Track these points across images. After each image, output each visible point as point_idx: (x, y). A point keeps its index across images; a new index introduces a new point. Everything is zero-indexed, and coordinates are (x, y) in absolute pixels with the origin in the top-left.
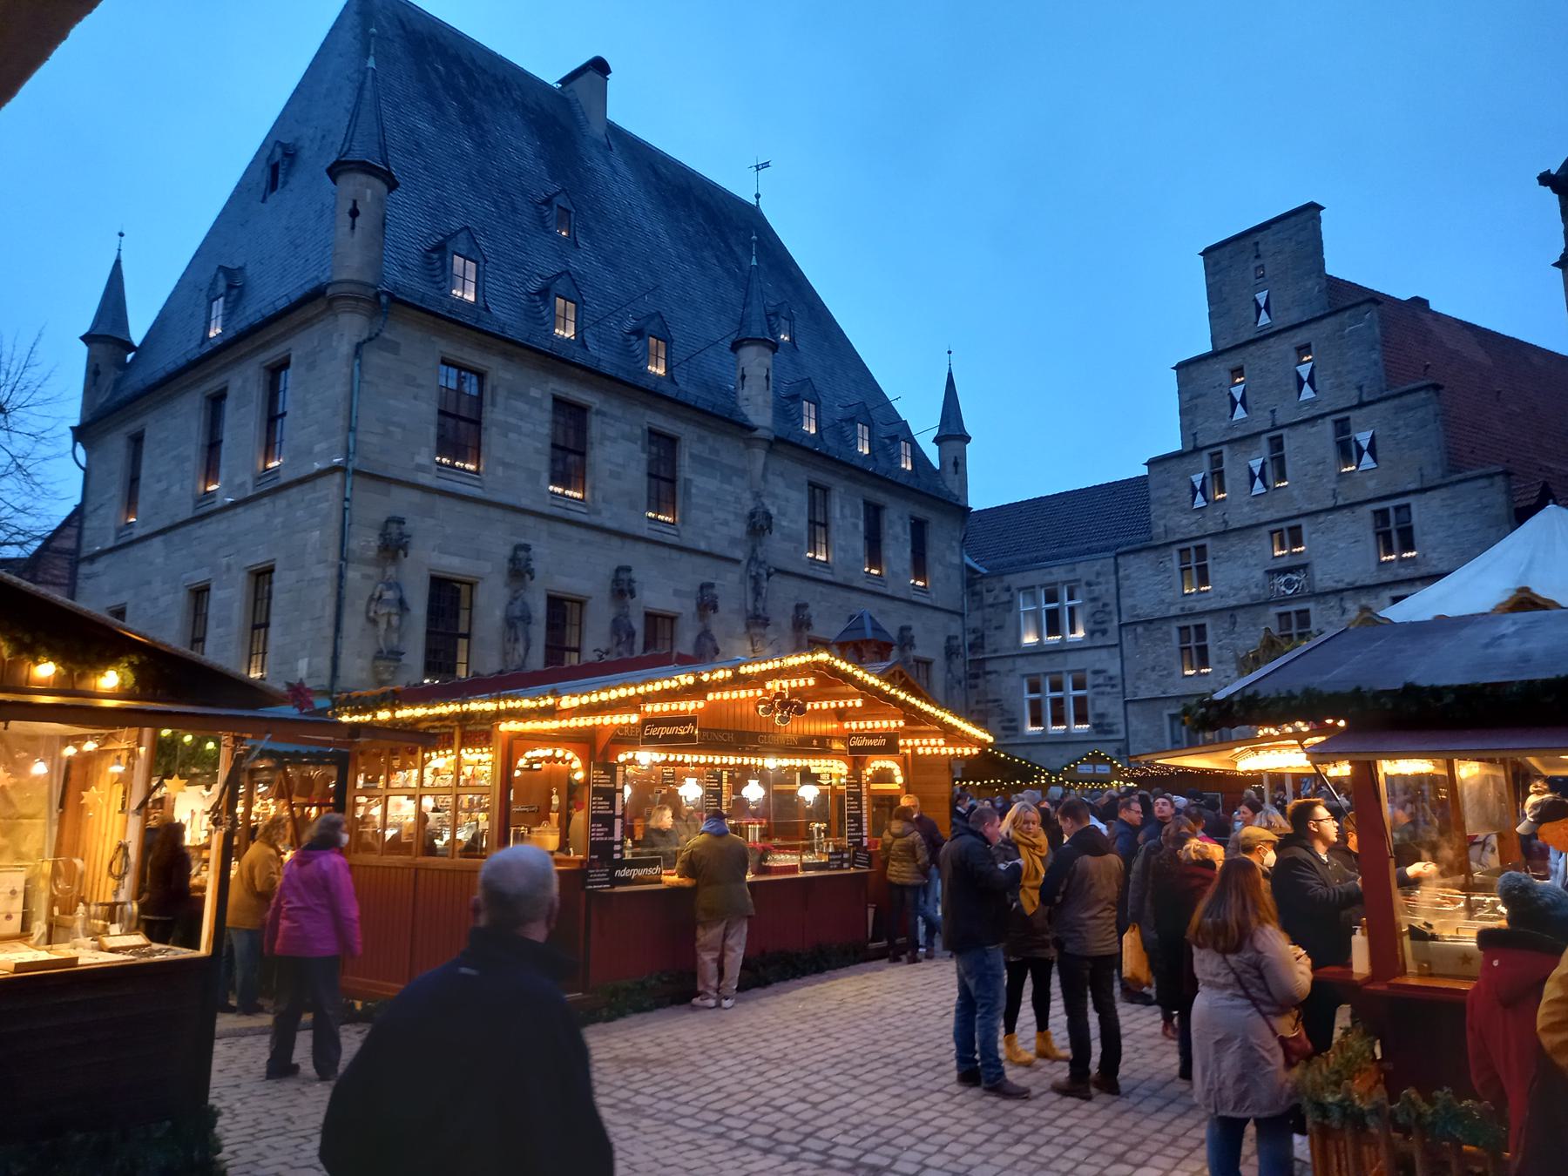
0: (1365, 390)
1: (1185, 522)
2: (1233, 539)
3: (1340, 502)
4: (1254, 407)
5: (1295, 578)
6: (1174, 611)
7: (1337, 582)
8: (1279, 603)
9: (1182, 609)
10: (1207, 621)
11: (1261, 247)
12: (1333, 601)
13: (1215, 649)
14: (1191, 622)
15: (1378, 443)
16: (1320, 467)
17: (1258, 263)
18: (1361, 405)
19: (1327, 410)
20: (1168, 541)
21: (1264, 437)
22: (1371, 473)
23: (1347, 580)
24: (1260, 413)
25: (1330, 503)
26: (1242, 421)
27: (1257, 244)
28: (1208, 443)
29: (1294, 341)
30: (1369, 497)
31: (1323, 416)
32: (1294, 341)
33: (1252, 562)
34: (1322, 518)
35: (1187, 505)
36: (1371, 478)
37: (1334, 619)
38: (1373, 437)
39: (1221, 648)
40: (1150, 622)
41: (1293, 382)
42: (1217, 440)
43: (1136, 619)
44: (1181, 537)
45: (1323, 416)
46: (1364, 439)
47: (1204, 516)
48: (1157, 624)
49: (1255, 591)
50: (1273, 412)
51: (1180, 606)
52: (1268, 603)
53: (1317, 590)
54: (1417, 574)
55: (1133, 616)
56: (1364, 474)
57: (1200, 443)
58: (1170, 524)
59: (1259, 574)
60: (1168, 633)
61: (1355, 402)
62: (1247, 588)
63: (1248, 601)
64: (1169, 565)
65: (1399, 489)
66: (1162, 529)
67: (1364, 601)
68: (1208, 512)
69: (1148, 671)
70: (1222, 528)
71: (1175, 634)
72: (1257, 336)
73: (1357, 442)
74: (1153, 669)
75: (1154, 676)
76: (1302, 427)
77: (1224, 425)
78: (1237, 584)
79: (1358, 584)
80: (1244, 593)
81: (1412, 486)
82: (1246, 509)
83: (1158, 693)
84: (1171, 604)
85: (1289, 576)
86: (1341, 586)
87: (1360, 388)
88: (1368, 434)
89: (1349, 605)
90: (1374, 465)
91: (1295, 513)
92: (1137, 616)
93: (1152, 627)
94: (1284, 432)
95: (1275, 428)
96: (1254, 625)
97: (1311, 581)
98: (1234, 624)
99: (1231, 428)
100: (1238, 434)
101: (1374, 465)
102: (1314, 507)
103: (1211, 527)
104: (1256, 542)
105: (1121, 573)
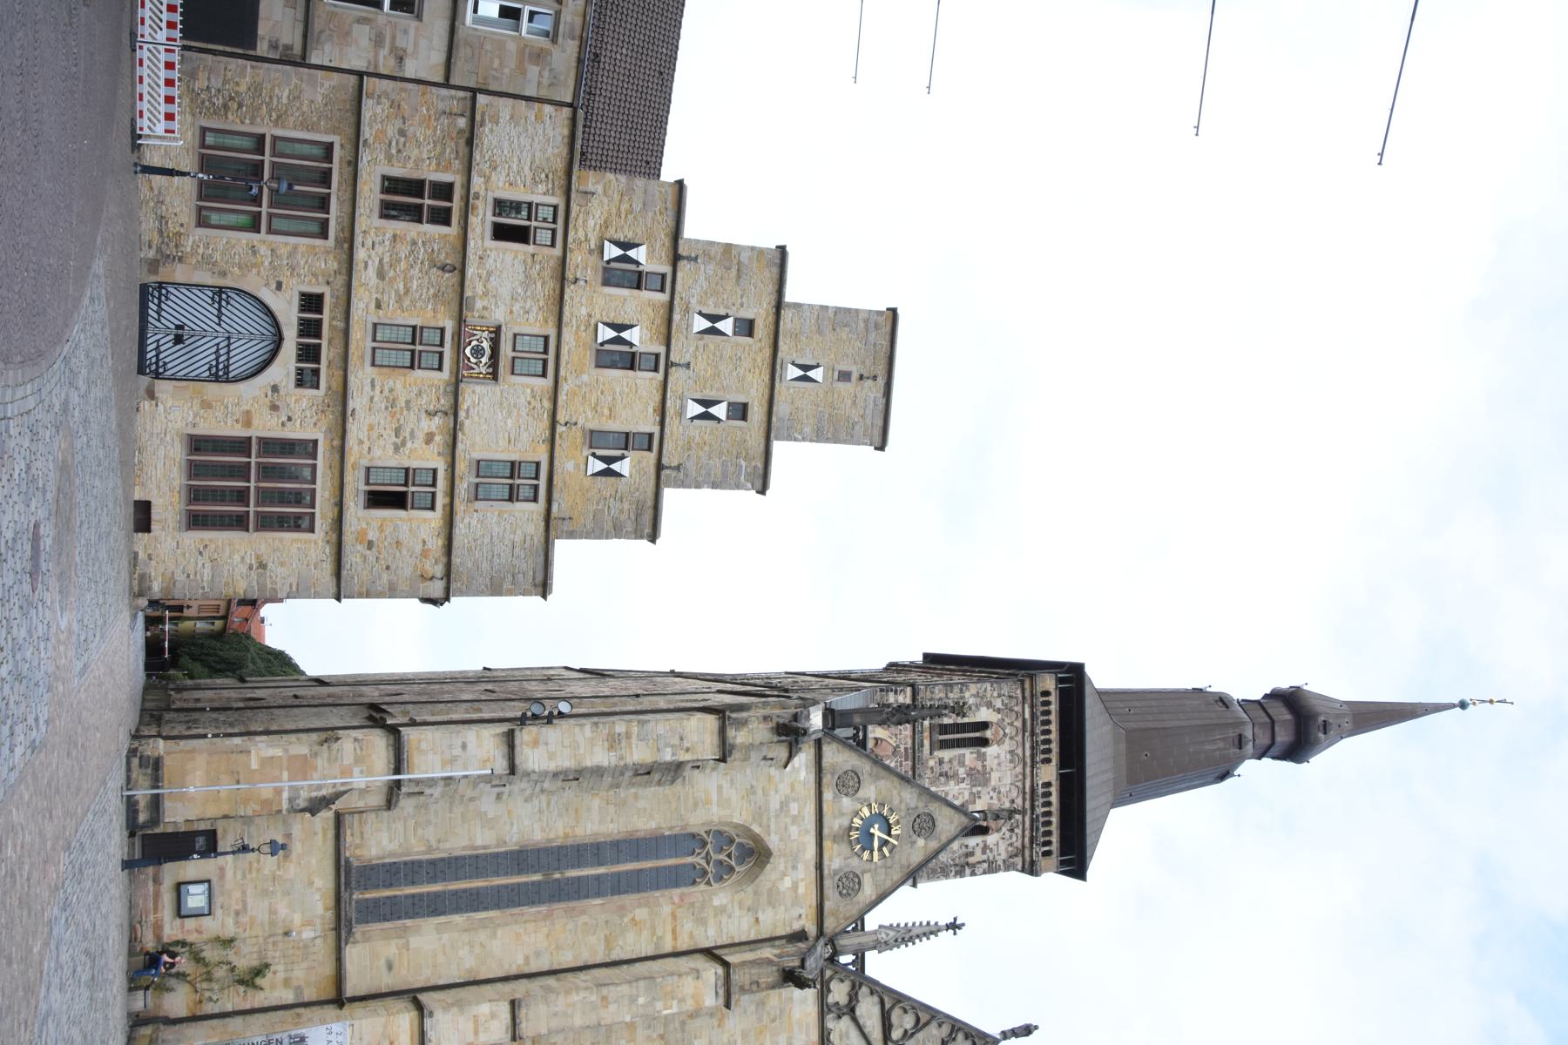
0: (674, 474)
1: (591, 223)
2: (552, 285)
3: (560, 429)
4: (701, 343)
5: (484, 360)
6: (477, 183)
7: (467, 411)
8: (458, 334)
9: (477, 197)
10: (453, 230)
11: (870, 383)
12: (445, 403)
13: (413, 234)
14: (456, 205)
15: (613, 479)
16: (606, 412)
17: (855, 376)
18: (659, 467)
19: (667, 430)
20: (573, 195)
21: (662, 350)
22: (583, 467)
23: (467, 422)
24: (692, 349)
25: (561, 417)
26: (689, 326)
27: (875, 378)
28: (679, 275)
29: (756, 403)
30: (556, 463)
31: (662, 424)
32: (756, 403)
33: (516, 308)
34: (547, 404)
35: (611, 233)
36: (577, 466)
37: (424, 400)
38: (620, 475)
39: (414, 243)
40: (470, 142)
41: (709, 394)
42: (678, 287)
43: (478, 118)
44: (573, 215)
45: (662, 424)
46: (622, 467)
47: (591, 252)
48: (463, 149)
49: (479, 304)
50: (688, 365)
51: (482, 193)
52: (461, 320)
53: (462, 385)
54: (457, 501)
55: (483, 114)
56: (583, 460)
57: (682, 264)
58: (595, 201)
59: (498, 315)
60: (447, 169)
61: (665, 461)
62: (485, 294)
63: (468, 293)
64: (542, 188)
65: (556, 495)
66: (590, 188)
67: (437, 438)
68: (594, 259)
69: (398, 123)
70: (569, 275)
71: (446, 177)
72: (779, 361)
73: (622, 458)
74: (402, 133)
75: (391, 131)
76: (657, 397)
77: (694, 301)
78: (493, 282)
79: (460, 435)
80: (480, 289)
81: (555, 508)
82: (584, 311)
83: (367, 132)
84: (488, 179)
85: (488, 352)
86: (462, 414)
87: (678, 468)
88: (626, 472)
89: (437, 420)
90: (589, 473)
91: (562, 373)
92: (482, 124)
93: (462, 142)
94: (660, 376)
95: (669, 365)
96: (435, 295)
97: (477, 378)
98: (443, 268)
99: (687, 310)
100: (676, 317)
101: (589, 473)
102: (562, 398)
103: (576, 258)
104: (540, 317)
105: (548, 109)
